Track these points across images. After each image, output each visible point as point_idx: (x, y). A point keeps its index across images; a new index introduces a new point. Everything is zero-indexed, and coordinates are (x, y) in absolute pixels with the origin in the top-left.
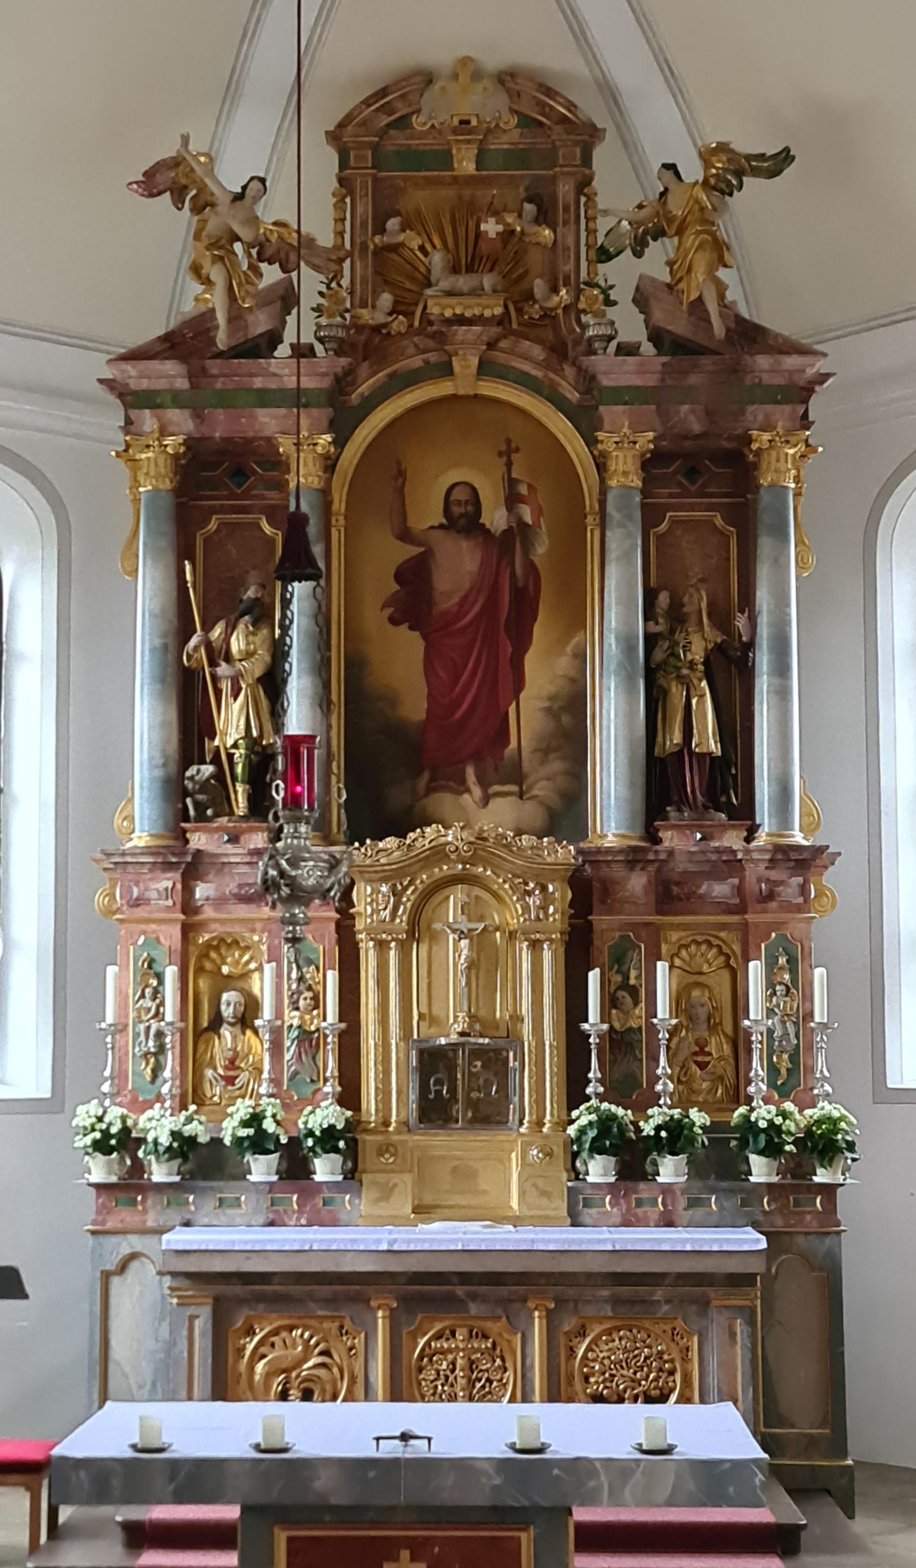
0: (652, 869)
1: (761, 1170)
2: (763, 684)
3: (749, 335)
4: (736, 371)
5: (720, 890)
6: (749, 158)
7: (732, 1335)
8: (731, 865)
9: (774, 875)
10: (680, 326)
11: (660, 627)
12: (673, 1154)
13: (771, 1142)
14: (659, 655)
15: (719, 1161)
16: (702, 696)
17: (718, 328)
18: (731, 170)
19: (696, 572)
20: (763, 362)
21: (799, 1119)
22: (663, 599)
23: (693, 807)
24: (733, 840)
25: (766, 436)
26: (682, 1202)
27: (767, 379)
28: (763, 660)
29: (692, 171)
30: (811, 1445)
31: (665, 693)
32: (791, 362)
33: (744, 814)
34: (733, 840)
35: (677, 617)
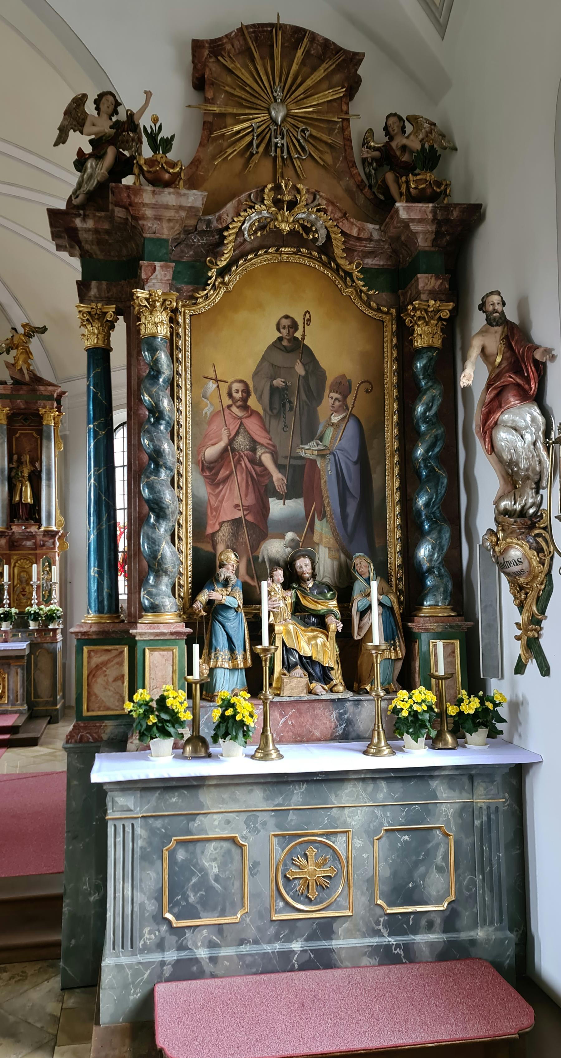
0: (8, 537)
1: (33, 625)
2: (44, 483)
3: (37, 380)
4: (34, 391)
5: (29, 543)
6: (35, 328)
7: (17, 673)
8: (32, 536)
9: (45, 539)
10: (18, 377)
11: (14, 465)
12: (5, 621)
13: (36, 616)
14: (13, 474)
15: (20, 623)
16: (26, 486)
17: (27, 378)
18: (33, 331)
19: (28, 448)
20: (42, 388)
21: (45, 609)
22: (15, 457)
23: (22, 519)
24: (33, 529)
25: (44, 410)
26: (10, 635)
27: (44, 393)
28: (44, 476)
29: (21, 330)
30: (47, 703)
31: (15, 485)
32: (50, 388)
33: (38, 522)
34: (33, 529)
35: (20, 462)
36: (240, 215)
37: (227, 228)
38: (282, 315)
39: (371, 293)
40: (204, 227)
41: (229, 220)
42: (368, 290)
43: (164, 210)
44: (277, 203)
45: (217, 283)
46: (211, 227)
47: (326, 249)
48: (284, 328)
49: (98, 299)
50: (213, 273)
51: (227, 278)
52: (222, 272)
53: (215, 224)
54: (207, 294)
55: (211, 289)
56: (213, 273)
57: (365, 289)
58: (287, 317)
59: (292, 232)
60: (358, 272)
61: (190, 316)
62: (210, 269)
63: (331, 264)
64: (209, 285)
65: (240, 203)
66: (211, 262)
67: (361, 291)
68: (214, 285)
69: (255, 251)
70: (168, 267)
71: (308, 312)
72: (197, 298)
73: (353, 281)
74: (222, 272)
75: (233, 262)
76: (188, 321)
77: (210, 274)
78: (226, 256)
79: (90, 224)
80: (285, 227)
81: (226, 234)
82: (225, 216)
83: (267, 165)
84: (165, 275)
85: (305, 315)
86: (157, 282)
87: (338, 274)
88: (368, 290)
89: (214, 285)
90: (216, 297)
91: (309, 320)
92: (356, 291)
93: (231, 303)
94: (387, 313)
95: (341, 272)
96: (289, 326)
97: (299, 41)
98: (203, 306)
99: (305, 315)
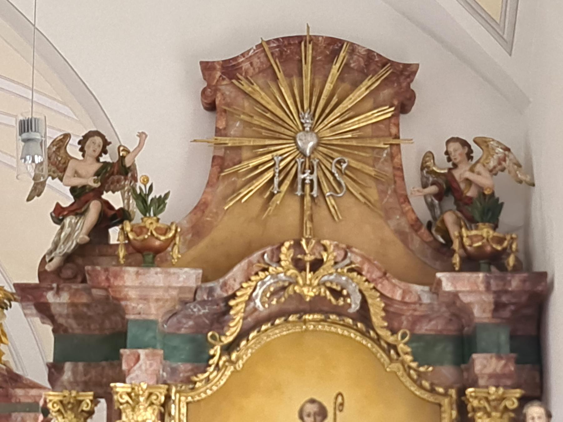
36: (250, 280)
37: (234, 296)
38: (307, 398)
39: (422, 369)
40: (205, 297)
41: (237, 286)
42: (419, 366)
43: (148, 292)
44: (299, 265)
45: (221, 363)
46: (213, 296)
47: (363, 315)
48: (309, 415)
49: (74, 384)
50: (216, 350)
51: (234, 356)
52: (228, 349)
53: (219, 293)
54: (208, 377)
55: (214, 370)
56: (216, 350)
57: (414, 365)
58: (312, 401)
59: (318, 298)
60: (405, 344)
61: (188, 404)
62: (213, 346)
63: (369, 333)
64: (210, 366)
65: (250, 264)
66: (213, 337)
67: (410, 368)
68: (217, 365)
69: (270, 318)
70: (154, 355)
71: (340, 394)
72: (195, 383)
73: (398, 354)
74: (228, 349)
75: (243, 335)
76: (184, 410)
77: (212, 352)
78: (233, 330)
79: (65, 298)
80: (309, 293)
81: (232, 303)
82: (231, 282)
83: (293, 205)
84: (151, 365)
85: (336, 398)
86: (142, 370)
87: (380, 346)
88: (419, 366)
89: (217, 365)
90: (220, 379)
91: (342, 404)
92: (403, 365)
93: (240, 385)
94: (446, 395)
95: (383, 343)
96: (315, 414)
97: (336, 53)
98: (204, 391)
99: (336, 398)
